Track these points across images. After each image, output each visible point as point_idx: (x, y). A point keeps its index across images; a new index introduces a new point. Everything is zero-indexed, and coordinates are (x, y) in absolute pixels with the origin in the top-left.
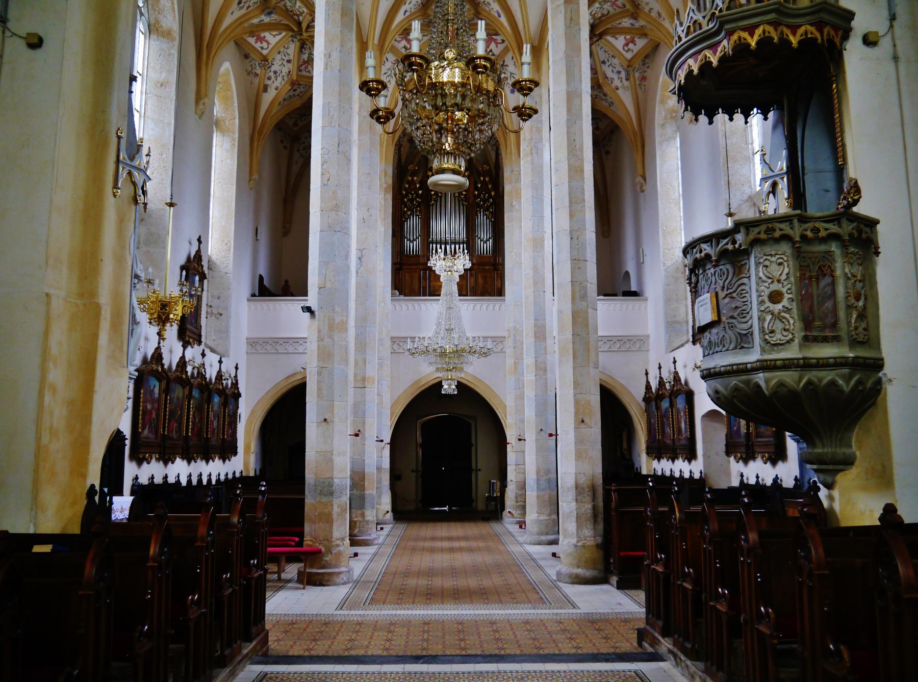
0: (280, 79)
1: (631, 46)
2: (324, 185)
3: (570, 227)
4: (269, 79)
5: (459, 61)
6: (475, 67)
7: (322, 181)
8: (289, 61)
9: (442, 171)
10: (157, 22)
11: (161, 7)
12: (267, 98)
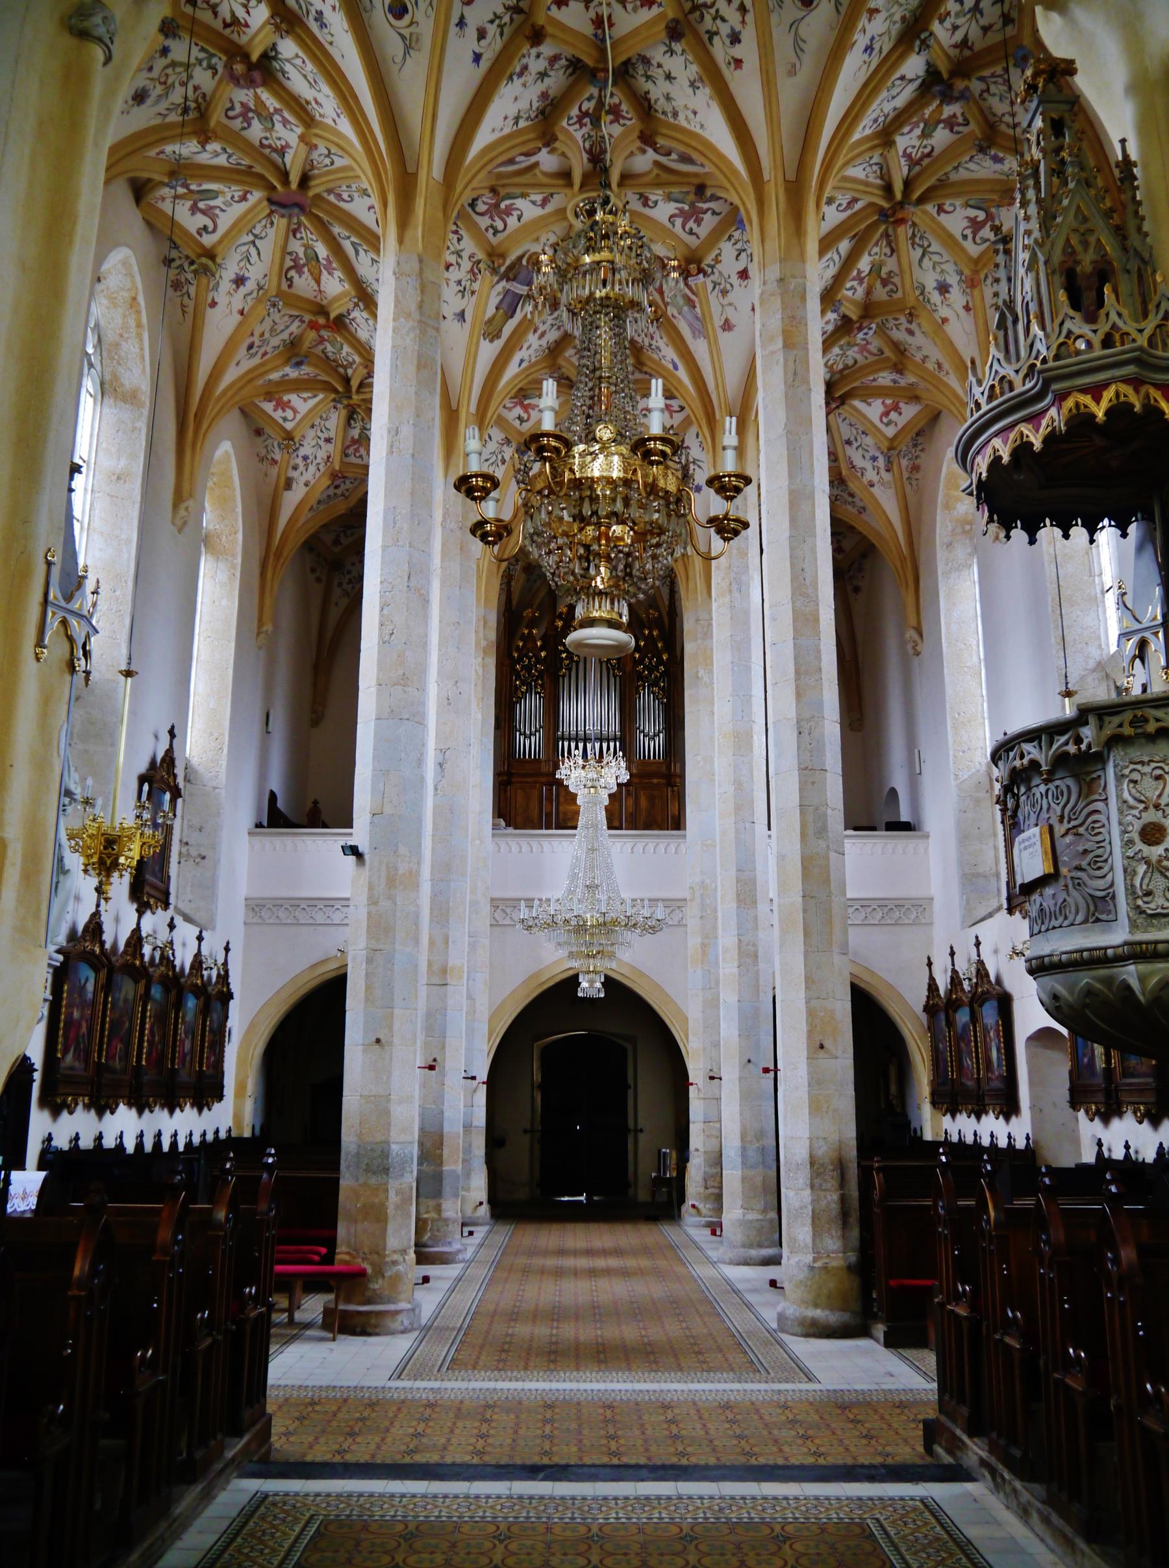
0: (312, 469)
2: (383, 642)
3: (798, 714)
4: (295, 468)
5: (620, 444)
6: (647, 454)
7: (380, 635)
8: (328, 440)
9: (590, 623)
10: (116, 377)
11: (123, 354)
12: (291, 500)
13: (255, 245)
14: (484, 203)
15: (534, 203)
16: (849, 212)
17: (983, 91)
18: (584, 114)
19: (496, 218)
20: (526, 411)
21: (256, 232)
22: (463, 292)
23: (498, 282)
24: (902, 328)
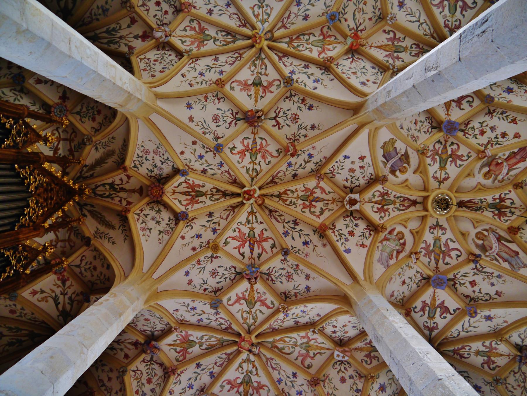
1: (228, 387)
8: (210, 12)
13: (416, 21)
14: (439, 148)
15: (436, 172)
16: (423, 328)
17: (514, 371)
18: (502, 200)
19: (431, 153)
20: (239, 153)
21: (424, 25)
22: (408, 130)
23: (406, 151)
24: (341, 374)
